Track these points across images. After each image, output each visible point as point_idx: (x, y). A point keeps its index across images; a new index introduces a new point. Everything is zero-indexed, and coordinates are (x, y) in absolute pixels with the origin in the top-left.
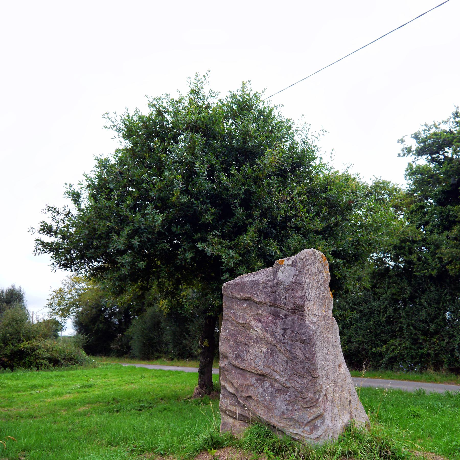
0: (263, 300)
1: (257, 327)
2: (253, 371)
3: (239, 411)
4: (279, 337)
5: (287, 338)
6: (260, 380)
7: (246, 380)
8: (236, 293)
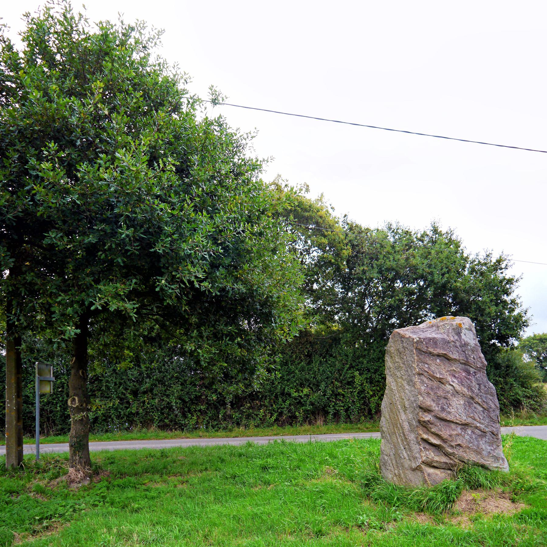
0: (457, 358)
1: (453, 382)
2: (458, 422)
3: (444, 459)
4: (476, 391)
5: (483, 391)
6: (463, 429)
7: (454, 430)
8: (432, 348)
